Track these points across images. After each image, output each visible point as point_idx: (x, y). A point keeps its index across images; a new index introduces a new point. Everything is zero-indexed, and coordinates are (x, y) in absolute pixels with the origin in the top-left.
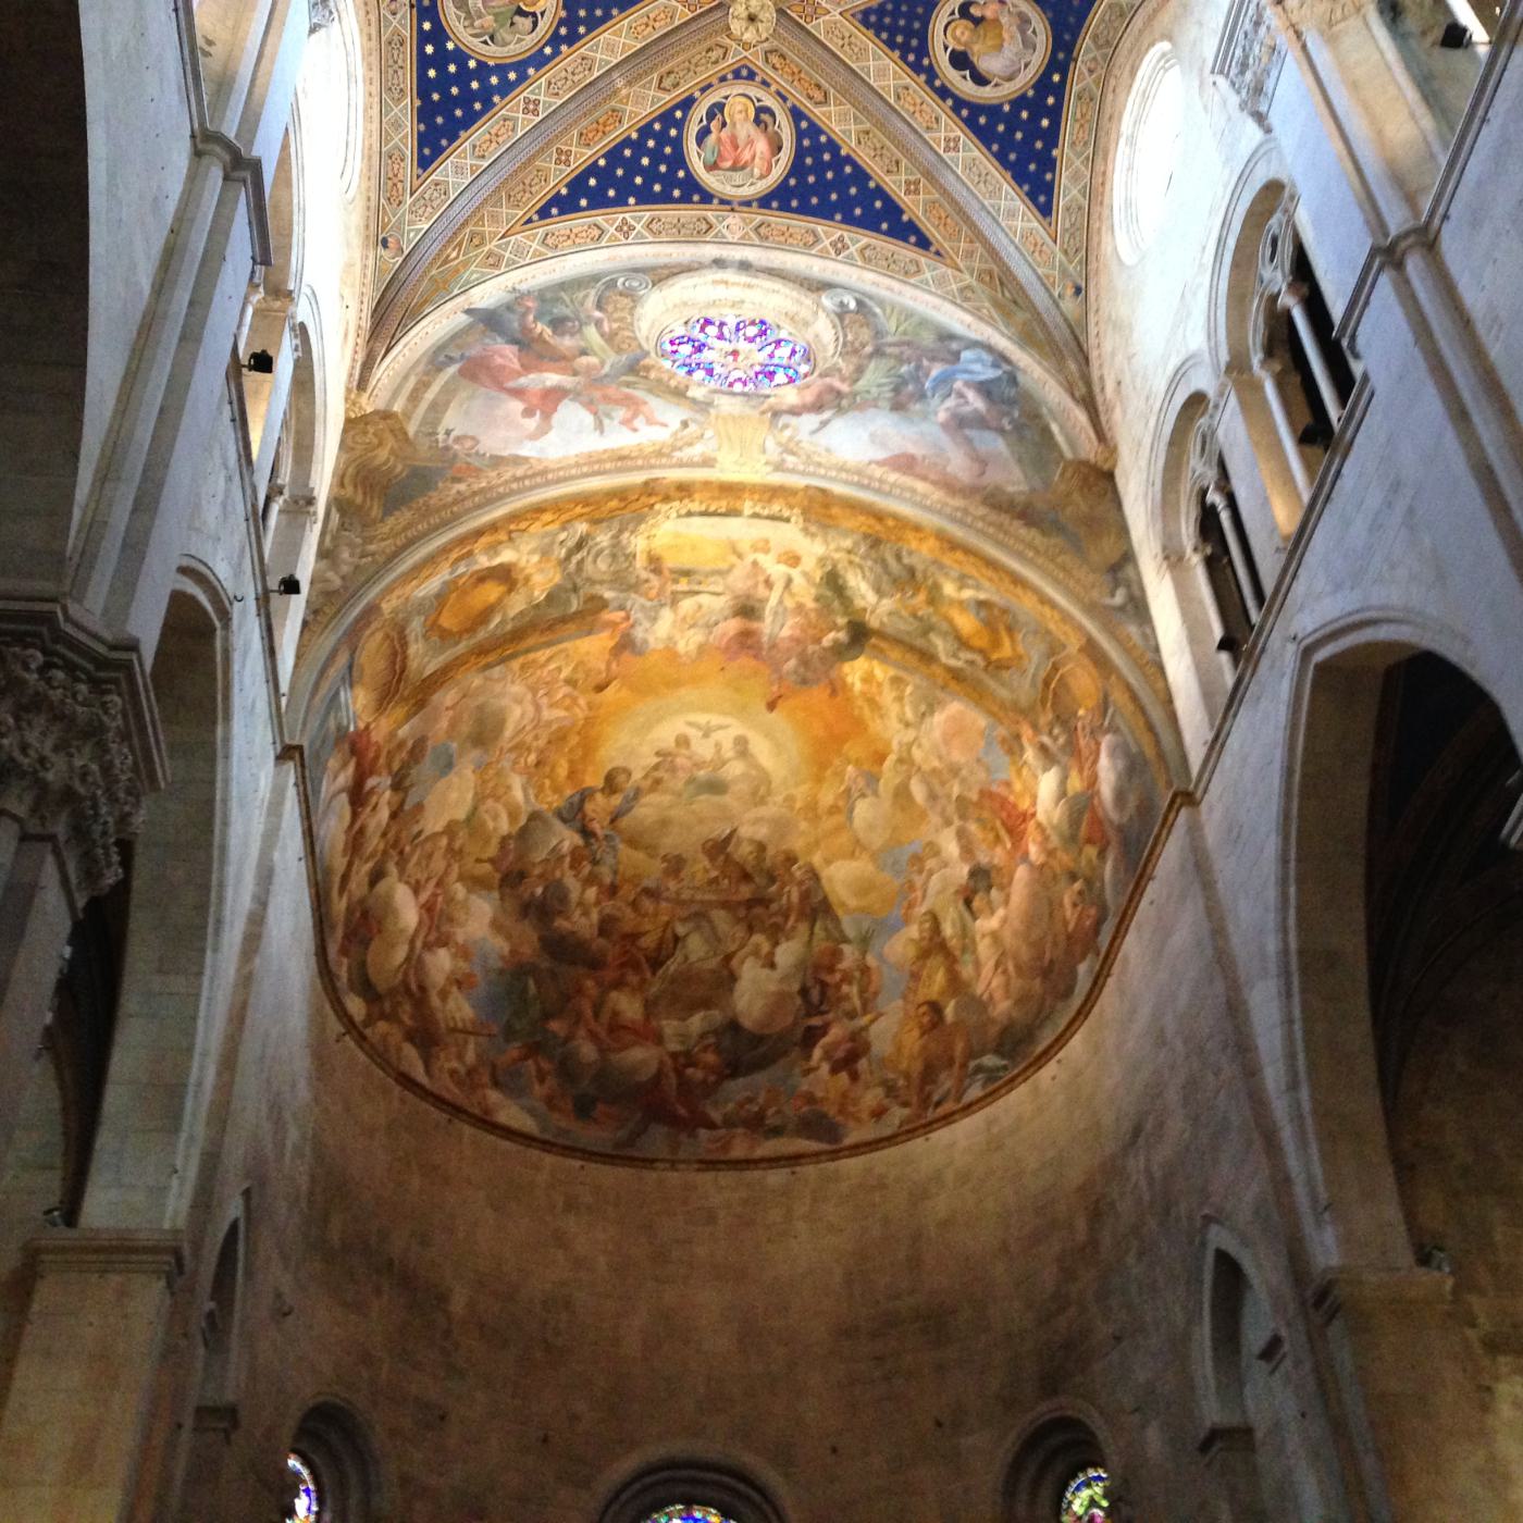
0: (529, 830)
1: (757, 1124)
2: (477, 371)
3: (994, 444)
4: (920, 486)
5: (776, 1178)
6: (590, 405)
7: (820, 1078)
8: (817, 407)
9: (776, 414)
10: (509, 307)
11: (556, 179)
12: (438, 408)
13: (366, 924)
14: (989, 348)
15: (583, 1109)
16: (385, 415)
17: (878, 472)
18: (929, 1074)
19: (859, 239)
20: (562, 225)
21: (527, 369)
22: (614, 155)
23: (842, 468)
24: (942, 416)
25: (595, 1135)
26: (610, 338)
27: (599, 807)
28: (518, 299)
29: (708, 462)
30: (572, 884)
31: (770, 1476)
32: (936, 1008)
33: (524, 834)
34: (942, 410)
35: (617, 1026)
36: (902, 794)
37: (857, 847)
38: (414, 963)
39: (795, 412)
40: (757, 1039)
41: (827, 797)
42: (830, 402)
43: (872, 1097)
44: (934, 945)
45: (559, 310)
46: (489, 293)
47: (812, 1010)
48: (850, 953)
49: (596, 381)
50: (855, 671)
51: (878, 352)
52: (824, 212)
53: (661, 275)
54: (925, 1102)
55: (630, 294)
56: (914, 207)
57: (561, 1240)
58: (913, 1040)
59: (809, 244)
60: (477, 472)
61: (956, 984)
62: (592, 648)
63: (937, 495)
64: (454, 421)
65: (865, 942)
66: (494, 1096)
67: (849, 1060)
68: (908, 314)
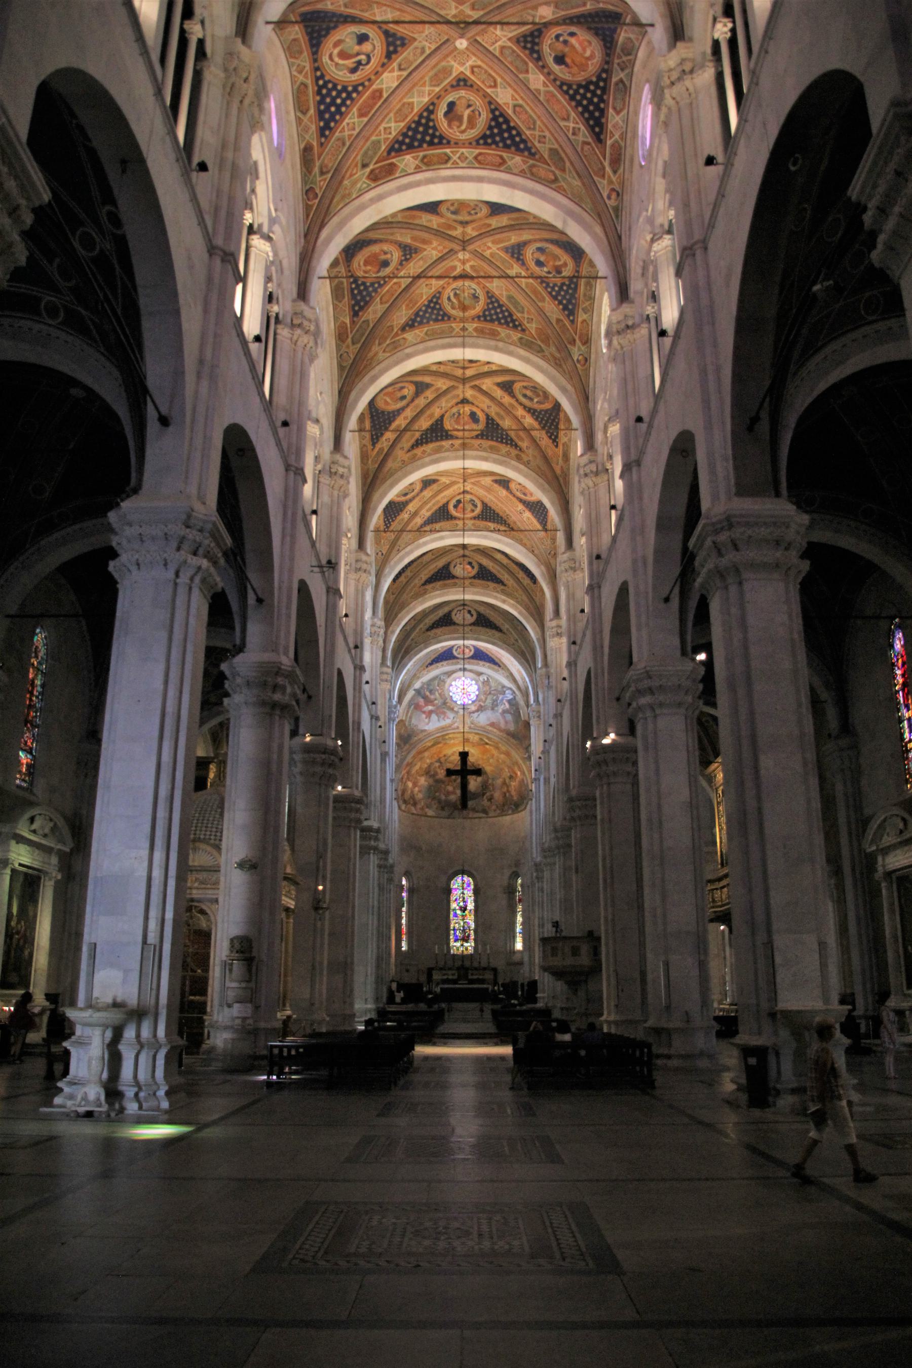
0: (430, 766)
1: (474, 810)
2: (417, 707)
3: (509, 717)
4: (495, 730)
5: (477, 820)
6: (437, 715)
7: (485, 803)
8: (477, 711)
9: (470, 713)
10: (422, 687)
11: (429, 661)
12: (411, 718)
13: (404, 792)
14: (510, 689)
15: (443, 809)
16: (401, 721)
17: (488, 727)
18: (504, 805)
19: (488, 664)
20: (430, 668)
21: (426, 705)
22: (439, 655)
23: (481, 727)
24: (500, 711)
25: (445, 813)
26: (440, 694)
27: (443, 760)
28: (423, 684)
29: (458, 728)
30: (439, 771)
31: (475, 873)
32: (505, 794)
33: (429, 766)
34: (500, 709)
35: (448, 793)
36: (498, 761)
37: (491, 765)
38: (412, 792)
39: (473, 712)
40: (474, 794)
41: (485, 757)
42: (481, 709)
43: (494, 807)
44: (504, 783)
45: (431, 687)
46: (417, 685)
47: (484, 789)
48: (490, 781)
49: (438, 708)
50: (487, 747)
51: (490, 693)
52: (481, 660)
53: (449, 674)
54: (503, 811)
55: (444, 681)
56: (497, 660)
57: (440, 834)
58: (501, 798)
59: (478, 664)
60: (418, 734)
61: (508, 791)
62: (440, 745)
63: (498, 732)
64: (414, 721)
65: (493, 779)
66: (427, 810)
67: (490, 799)
68: (496, 681)
